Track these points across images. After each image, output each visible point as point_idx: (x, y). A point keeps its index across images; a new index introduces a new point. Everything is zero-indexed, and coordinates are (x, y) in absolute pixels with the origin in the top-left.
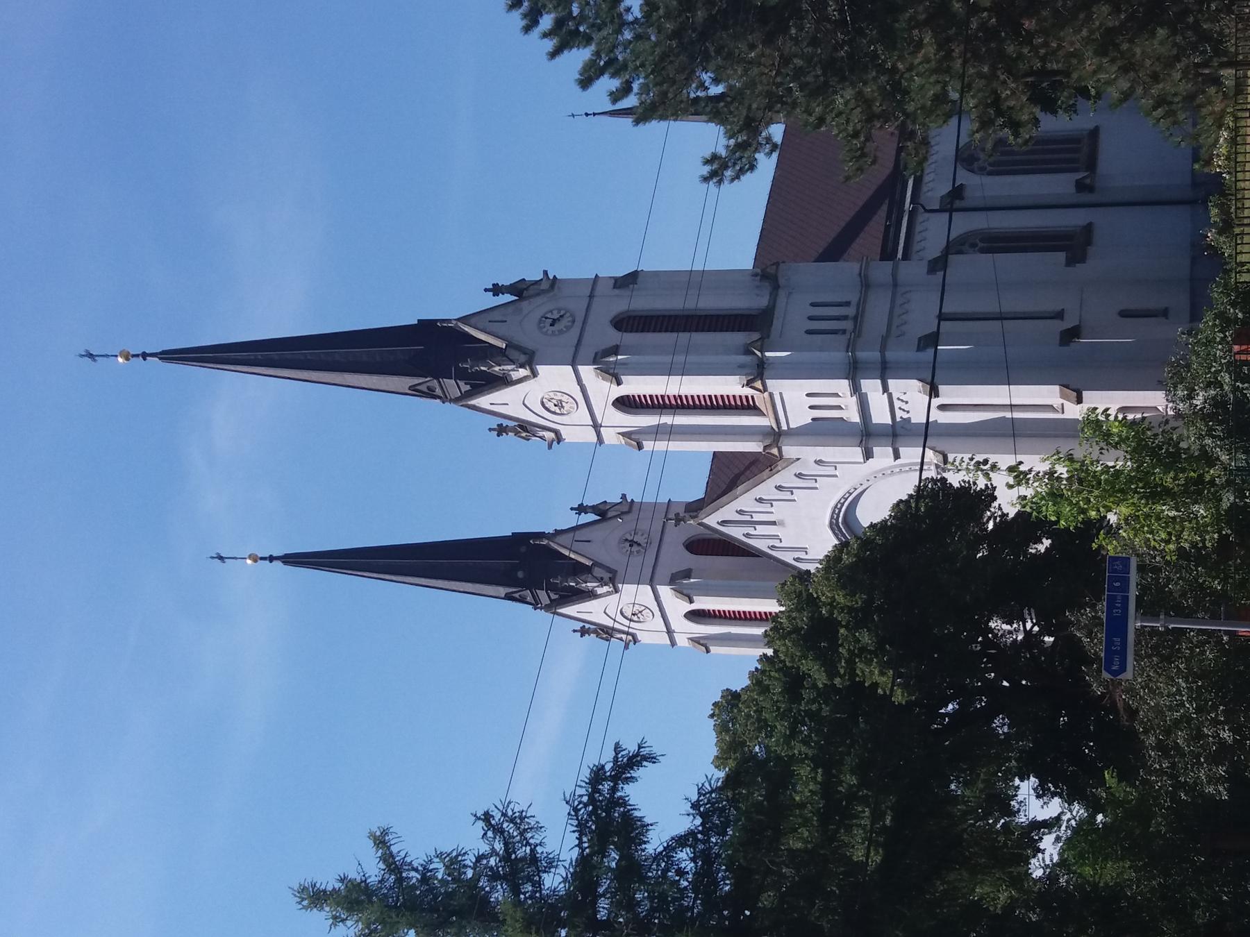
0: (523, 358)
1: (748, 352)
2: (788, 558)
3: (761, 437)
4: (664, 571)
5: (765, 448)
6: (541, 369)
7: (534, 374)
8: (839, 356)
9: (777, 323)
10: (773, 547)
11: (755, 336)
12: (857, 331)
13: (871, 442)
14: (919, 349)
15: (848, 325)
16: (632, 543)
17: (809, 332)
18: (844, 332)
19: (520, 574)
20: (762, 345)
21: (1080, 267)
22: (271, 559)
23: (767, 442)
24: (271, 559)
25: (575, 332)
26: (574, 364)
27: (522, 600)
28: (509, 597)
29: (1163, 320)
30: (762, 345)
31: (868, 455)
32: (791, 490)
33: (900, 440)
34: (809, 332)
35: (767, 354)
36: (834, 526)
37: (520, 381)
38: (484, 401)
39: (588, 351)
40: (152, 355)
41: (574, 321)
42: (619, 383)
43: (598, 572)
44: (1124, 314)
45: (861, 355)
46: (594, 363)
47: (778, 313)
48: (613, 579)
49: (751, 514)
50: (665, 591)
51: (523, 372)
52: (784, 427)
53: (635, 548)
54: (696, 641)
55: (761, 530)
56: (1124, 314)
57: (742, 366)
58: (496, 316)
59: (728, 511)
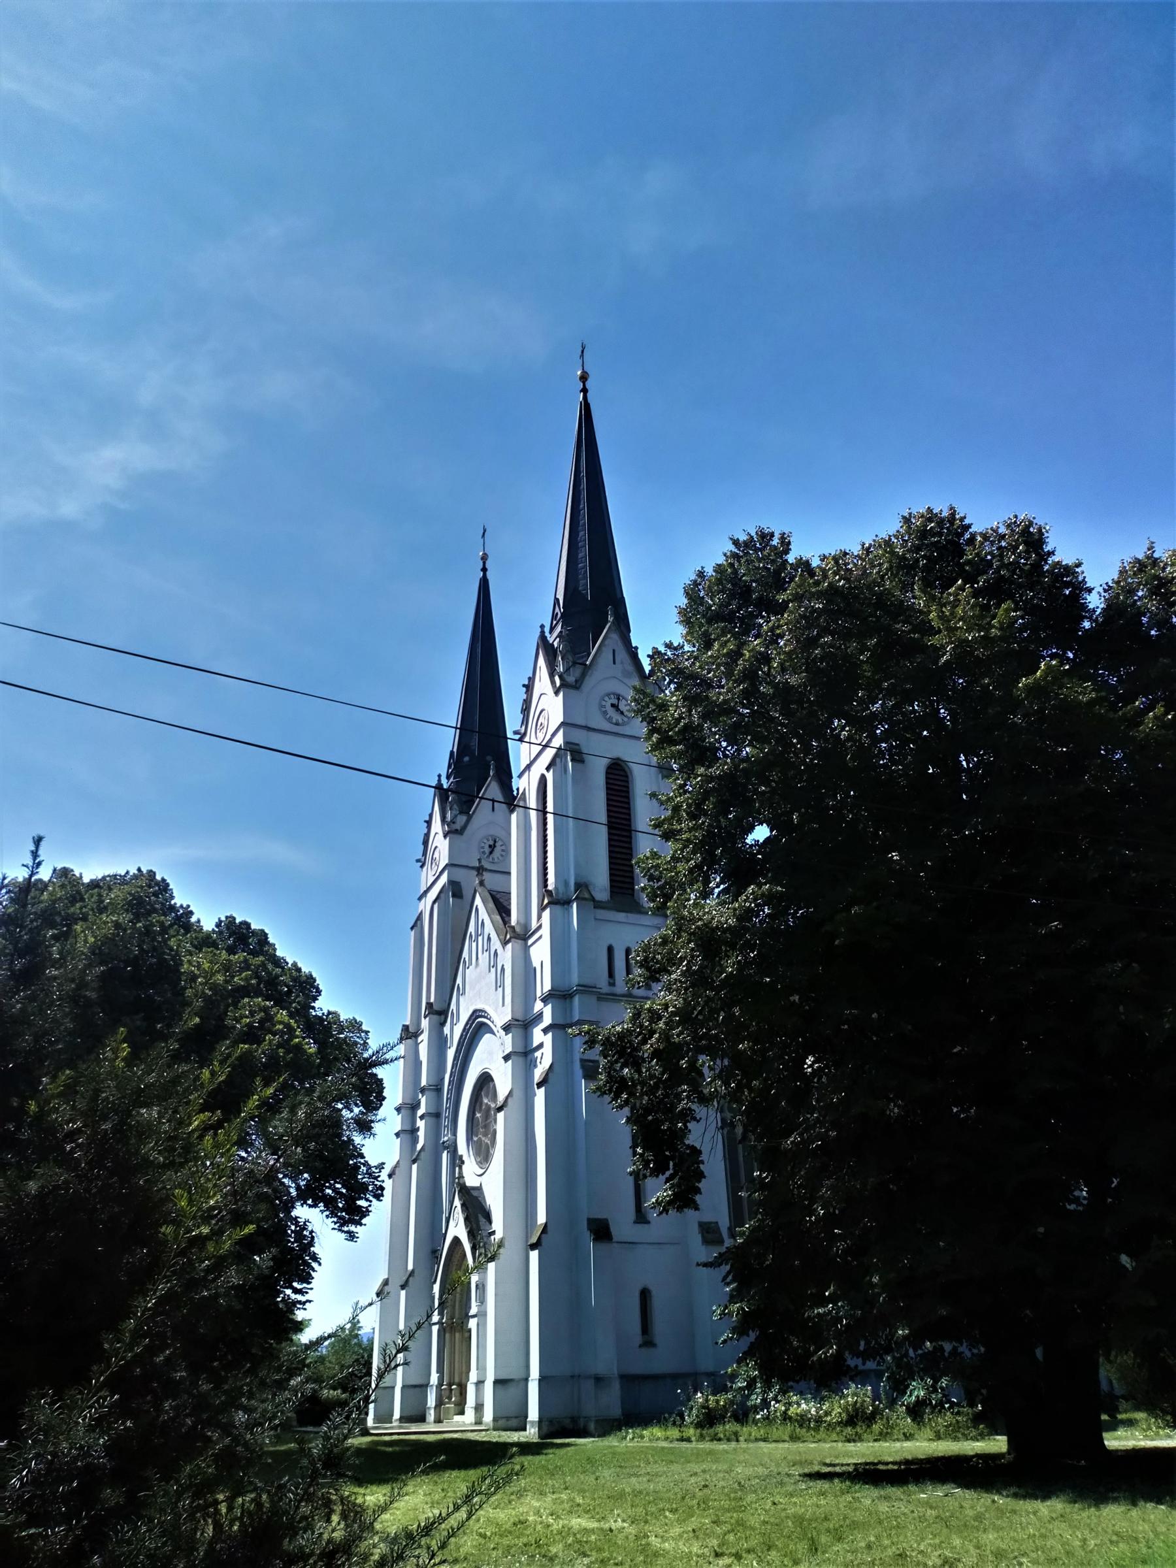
0: (571, 679)
1: (578, 886)
2: (459, 981)
3: (522, 921)
4: (461, 875)
5: (513, 928)
6: (561, 694)
7: (556, 693)
8: (575, 979)
9: (621, 916)
10: (465, 962)
11: (602, 894)
12: (602, 998)
13: (519, 1032)
14: (583, 1062)
15: (621, 987)
16: (492, 848)
17: (610, 950)
18: (612, 984)
19: (466, 759)
20: (585, 899)
21: (698, 1238)
22: (484, 570)
23: (518, 929)
24: (484, 570)
25: (606, 726)
26: (563, 724)
27: (449, 767)
28: (452, 753)
29: (638, 1339)
30: (585, 899)
31: (507, 1028)
32: (495, 966)
33: (520, 1060)
34: (610, 950)
35: (575, 905)
36: (477, 1014)
37: (553, 682)
38: (541, 661)
39: (579, 736)
40: (585, 398)
41: (617, 724)
42: (548, 769)
43: (462, 819)
44: (645, 1295)
45: (576, 999)
46: (566, 743)
47: (633, 917)
48: (452, 832)
49: (482, 934)
50: (444, 879)
51: (558, 683)
52: (530, 942)
53: (487, 850)
54: (420, 918)
55: (474, 944)
56: (645, 1295)
57: (566, 884)
58: (622, 655)
59: (483, 914)
